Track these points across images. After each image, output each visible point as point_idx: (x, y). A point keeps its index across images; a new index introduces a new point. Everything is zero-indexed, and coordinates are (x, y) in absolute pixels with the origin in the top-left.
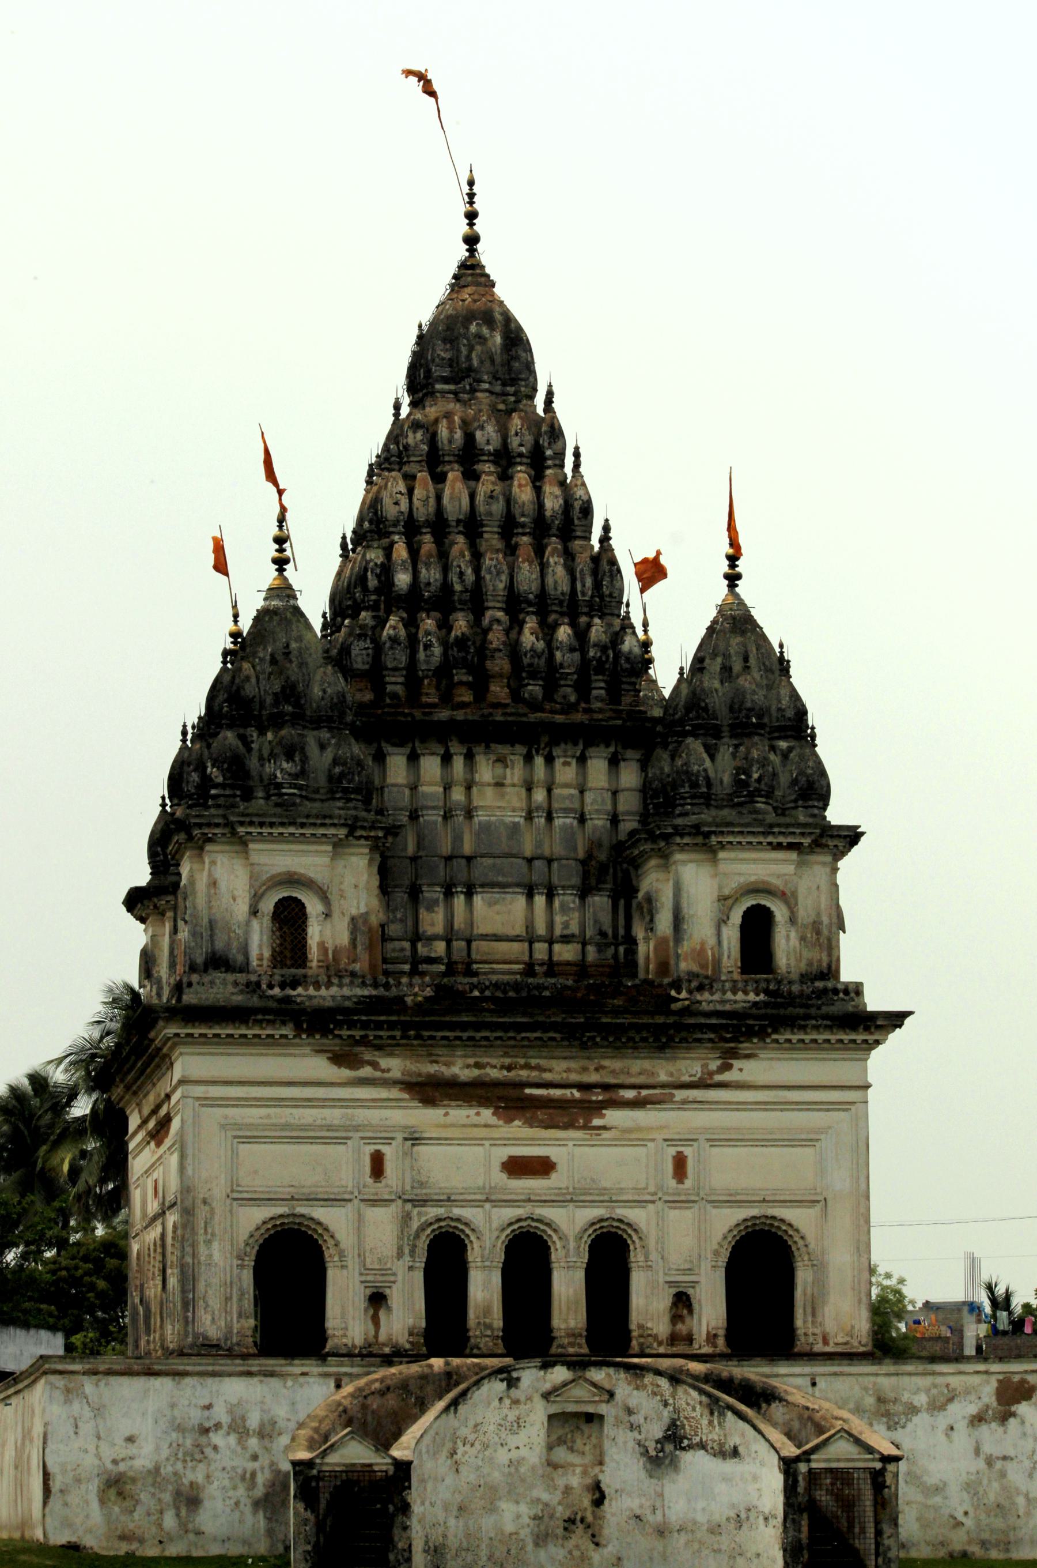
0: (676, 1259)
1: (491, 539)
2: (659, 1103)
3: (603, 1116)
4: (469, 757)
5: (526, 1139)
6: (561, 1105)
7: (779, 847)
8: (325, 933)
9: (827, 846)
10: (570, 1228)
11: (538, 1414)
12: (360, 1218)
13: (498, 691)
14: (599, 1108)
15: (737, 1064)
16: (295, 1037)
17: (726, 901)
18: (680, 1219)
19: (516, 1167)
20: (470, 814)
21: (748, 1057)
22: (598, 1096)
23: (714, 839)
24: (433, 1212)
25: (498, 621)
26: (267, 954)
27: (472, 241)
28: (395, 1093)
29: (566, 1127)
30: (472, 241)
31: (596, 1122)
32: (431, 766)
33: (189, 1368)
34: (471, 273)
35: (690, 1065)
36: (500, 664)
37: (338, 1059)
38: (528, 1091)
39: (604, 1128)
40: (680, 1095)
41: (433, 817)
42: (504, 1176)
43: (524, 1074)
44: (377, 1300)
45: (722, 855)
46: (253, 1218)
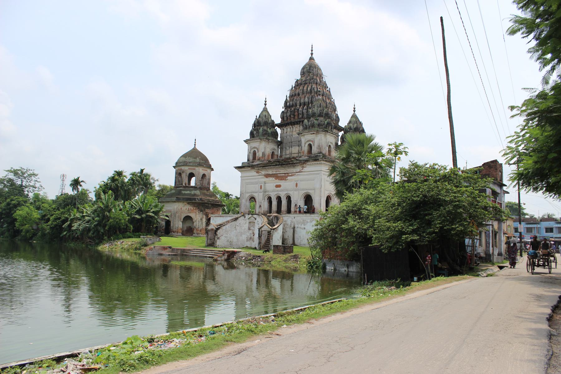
0: (295, 199)
1: (300, 96)
5: (278, 182)
8: (259, 154)
11: (248, 221)
13: (296, 117)
14: (287, 177)
18: (296, 193)
22: (287, 175)
24: (267, 193)
27: (312, 54)
28: (263, 176)
30: (312, 54)
32: (289, 129)
34: (311, 59)
35: (298, 169)
36: (296, 113)
37: (257, 172)
41: (288, 137)
43: (278, 173)
44: (260, 206)
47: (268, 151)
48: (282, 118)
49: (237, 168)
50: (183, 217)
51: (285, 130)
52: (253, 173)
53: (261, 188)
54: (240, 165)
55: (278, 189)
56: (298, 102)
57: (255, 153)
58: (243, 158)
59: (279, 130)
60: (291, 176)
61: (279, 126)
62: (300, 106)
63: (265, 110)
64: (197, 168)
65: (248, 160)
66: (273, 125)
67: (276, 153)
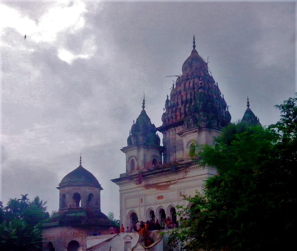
2: (177, 183)
3: (170, 187)
4: (175, 130)
6: (162, 186)
7: (193, 132)
9: (203, 130)
10: (166, 207)
12: (140, 210)
13: (178, 118)
14: (168, 186)
15: (187, 173)
16: (130, 181)
17: (187, 145)
19: (160, 198)
20: (175, 139)
21: (189, 172)
23: (184, 134)
24: (148, 207)
25: (180, 106)
26: (130, 169)
29: (165, 190)
31: (169, 188)
33: (100, 237)
35: (181, 175)
36: (178, 114)
38: (159, 184)
39: (170, 189)
40: (180, 181)
41: (171, 141)
42: (157, 199)
43: (159, 181)
45: (187, 136)
46: (128, 211)
47: (149, 159)
48: (164, 120)
49: (115, 181)
50: (68, 241)
51: (168, 134)
52: (132, 185)
53: (142, 202)
54: (119, 177)
55: (161, 201)
56: (180, 101)
57: (133, 163)
58: (121, 169)
59: (160, 135)
60: (174, 183)
61: (161, 129)
62: (182, 104)
63: (144, 113)
64: (82, 188)
65: (127, 171)
66: (153, 129)
67: (158, 161)
